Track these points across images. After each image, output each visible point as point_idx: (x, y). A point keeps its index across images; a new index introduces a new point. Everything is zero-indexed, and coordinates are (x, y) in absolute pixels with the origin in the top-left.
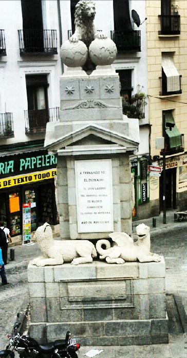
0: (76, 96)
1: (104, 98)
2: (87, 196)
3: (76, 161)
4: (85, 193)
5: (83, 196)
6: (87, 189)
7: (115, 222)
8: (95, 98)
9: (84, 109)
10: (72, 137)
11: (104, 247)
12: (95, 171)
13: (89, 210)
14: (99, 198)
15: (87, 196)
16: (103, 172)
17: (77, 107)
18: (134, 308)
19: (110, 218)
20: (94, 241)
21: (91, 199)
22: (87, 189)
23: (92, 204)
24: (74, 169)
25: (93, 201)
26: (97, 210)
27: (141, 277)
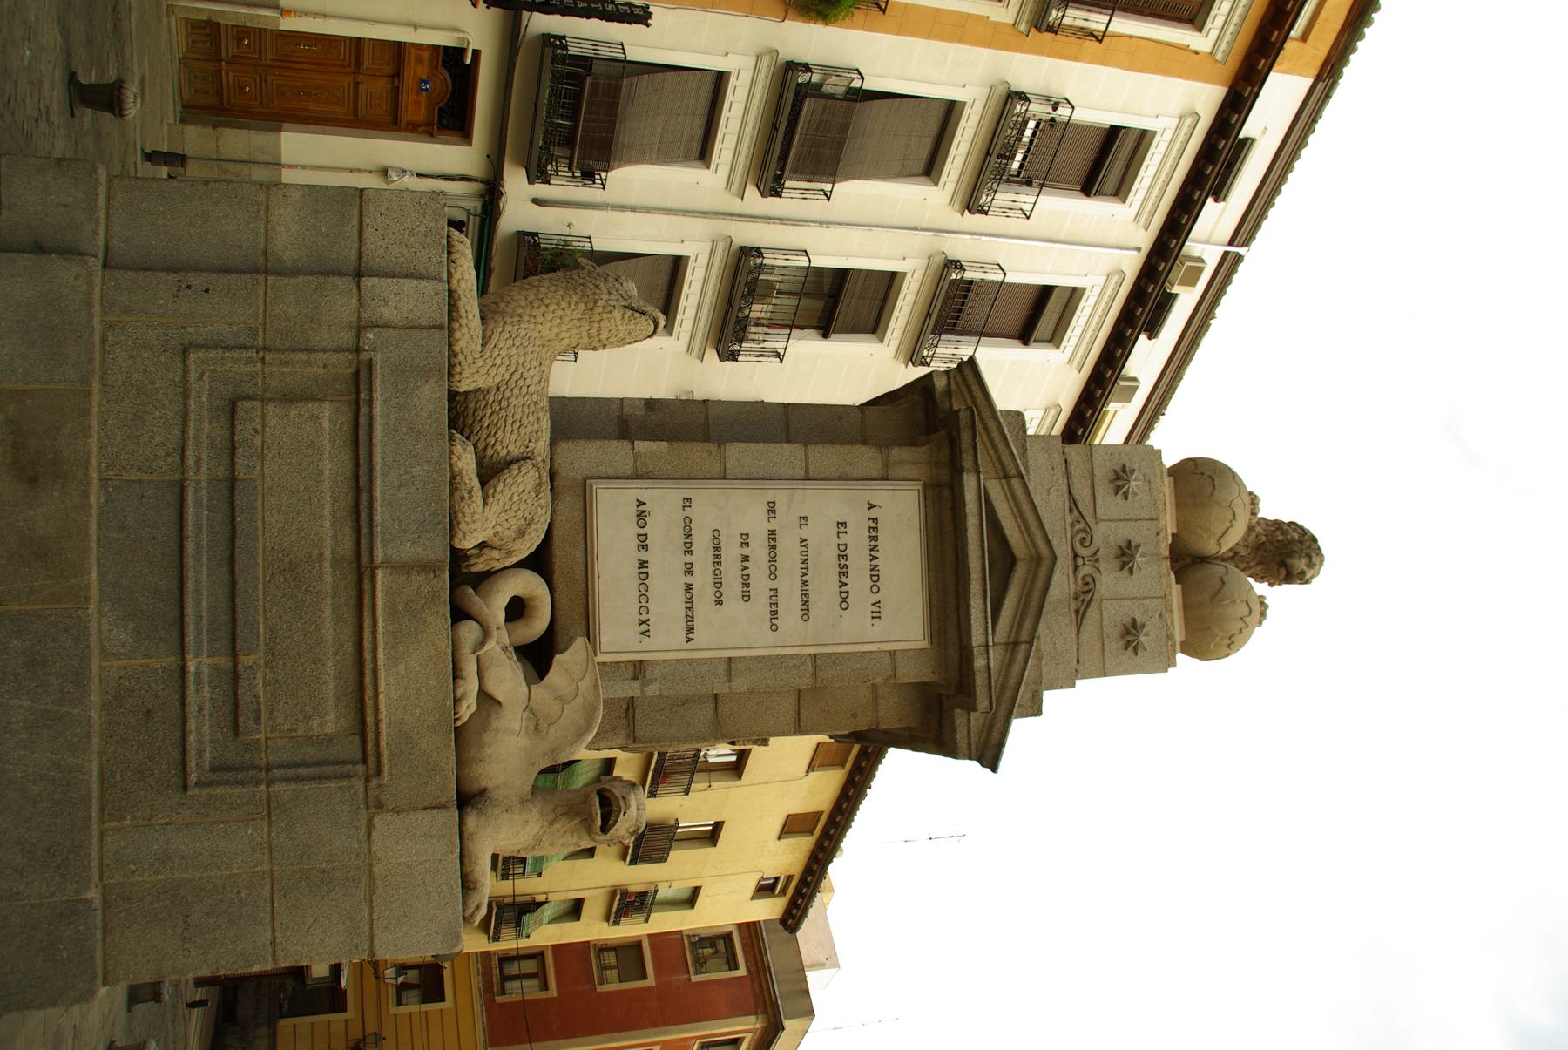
0: (1109, 504)
1: (1104, 613)
2: (772, 535)
3: (918, 486)
4: (785, 522)
5: (772, 510)
6: (804, 533)
7: (639, 670)
8: (1109, 581)
9: (1069, 535)
10: (1006, 477)
11: (517, 609)
12: (883, 571)
13: (702, 542)
14: (760, 586)
15: (772, 535)
16: (876, 615)
17: (1074, 505)
18: (185, 787)
19: (666, 642)
20: (539, 562)
21: (758, 550)
22: (804, 533)
23: (732, 552)
24: (885, 478)
25: (745, 558)
26: (702, 579)
27: (376, 820)
